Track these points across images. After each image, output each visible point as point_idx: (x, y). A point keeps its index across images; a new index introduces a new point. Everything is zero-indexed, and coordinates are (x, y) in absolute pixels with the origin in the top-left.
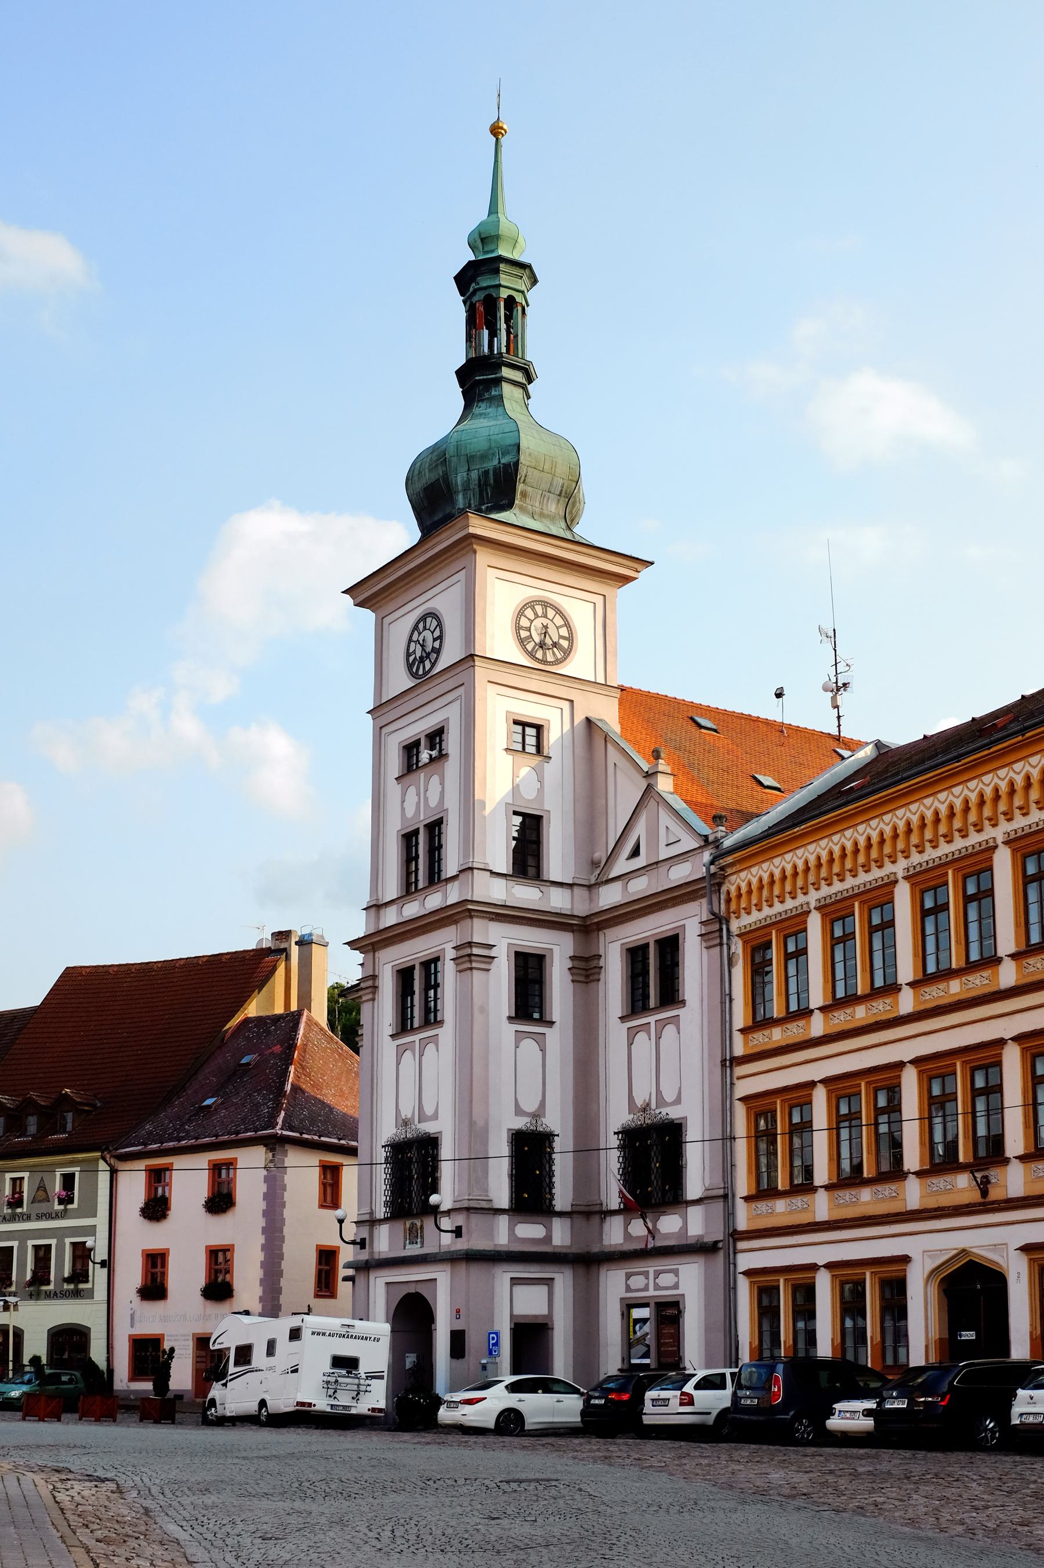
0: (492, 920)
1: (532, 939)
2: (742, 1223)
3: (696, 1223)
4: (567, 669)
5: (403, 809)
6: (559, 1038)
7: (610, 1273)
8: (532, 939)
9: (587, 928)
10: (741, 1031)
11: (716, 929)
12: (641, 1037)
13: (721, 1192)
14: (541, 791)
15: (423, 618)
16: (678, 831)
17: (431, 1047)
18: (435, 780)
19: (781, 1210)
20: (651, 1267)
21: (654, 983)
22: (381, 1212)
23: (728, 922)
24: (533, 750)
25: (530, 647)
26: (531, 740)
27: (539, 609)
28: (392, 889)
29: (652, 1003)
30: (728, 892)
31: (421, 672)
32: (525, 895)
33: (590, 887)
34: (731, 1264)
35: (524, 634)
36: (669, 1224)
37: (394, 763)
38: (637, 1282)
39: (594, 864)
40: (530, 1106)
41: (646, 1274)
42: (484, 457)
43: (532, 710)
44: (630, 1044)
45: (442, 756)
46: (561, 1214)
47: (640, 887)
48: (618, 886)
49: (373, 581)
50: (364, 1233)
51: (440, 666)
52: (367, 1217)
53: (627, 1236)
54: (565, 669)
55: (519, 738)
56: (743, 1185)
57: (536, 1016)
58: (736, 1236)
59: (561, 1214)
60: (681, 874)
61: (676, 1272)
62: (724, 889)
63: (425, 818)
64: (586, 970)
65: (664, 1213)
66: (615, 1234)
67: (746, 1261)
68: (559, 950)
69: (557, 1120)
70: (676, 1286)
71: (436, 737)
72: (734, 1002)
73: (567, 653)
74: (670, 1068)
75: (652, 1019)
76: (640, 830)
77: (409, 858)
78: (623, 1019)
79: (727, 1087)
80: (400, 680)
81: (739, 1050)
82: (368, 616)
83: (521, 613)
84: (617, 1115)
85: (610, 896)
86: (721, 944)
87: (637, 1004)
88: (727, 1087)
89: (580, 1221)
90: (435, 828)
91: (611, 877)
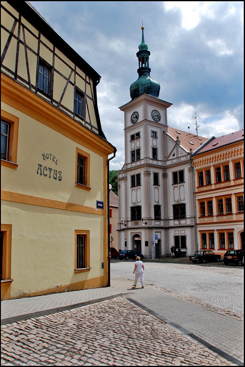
0: (150, 167)
1: (156, 171)
2: (198, 222)
3: (188, 222)
5: (131, 147)
6: (161, 188)
7: (171, 230)
8: (156, 171)
9: (165, 168)
10: (197, 188)
11: (191, 170)
12: (176, 188)
13: (194, 216)
14: (156, 144)
15: (134, 113)
16: (183, 152)
18: (138, 142)
19: (206, 220)
20: (180, 229)
21: (179, 178)
22: (130, 219)
23: (194, 168)
24: (154, 136)
26: (154, 135)
27: (155, 111)
28: (129, 161)
29: (178, 182)
30: (194, 163)
31: (134, 122)
32: (155, 162)
33: (165, 161)
34: (196, 230)
35: (153, 116)
36: (183, 222)
37: (129, 138)
38: (177, 232)
39: (166, 157)
40: (157, 201)
41: (179, 231)
42: (145, 84)
43: (155, 129)
44: (174, 189)
45: (139, 137)
46: (162, 220)
47: (175, 161)
48: (171, 161)
49: (125, 106)
50: (126, 223)
51: (138, 122)
52: (126, 220)
53: (174, 224)
54: (159, 122)
55: (152, 134)
56: (198, 214)
57: (157, 184)
58: (197, 224)
59: (162, 220)
60: (183, 159)
61: (185, 231)
62: (193, 162)
63: (136, 148)
64: (165, 176)
65: (182, 220)
66: (172, 223)
67: (199, 229)
68: (160, 173)
69: (161, 203)
70: (185, 233)
71: (138, 134)
72: (195, 183)
73: (160, 119)
74: (183, 193)
75: (178, 185)
76: (175, 151)
77: (133, 155)
78: (172, 185)
79: (194, 198)
80: (130, 124)
81: (197, 191)
82: (123, 112)
83: (152, 112)
84: (172, 203)
85: (169, 163)
86: (192, 172)
87: (175, 182)
88: (194, 198)
89: (165, 221)
90: (138, 151)
91: (169, 159)
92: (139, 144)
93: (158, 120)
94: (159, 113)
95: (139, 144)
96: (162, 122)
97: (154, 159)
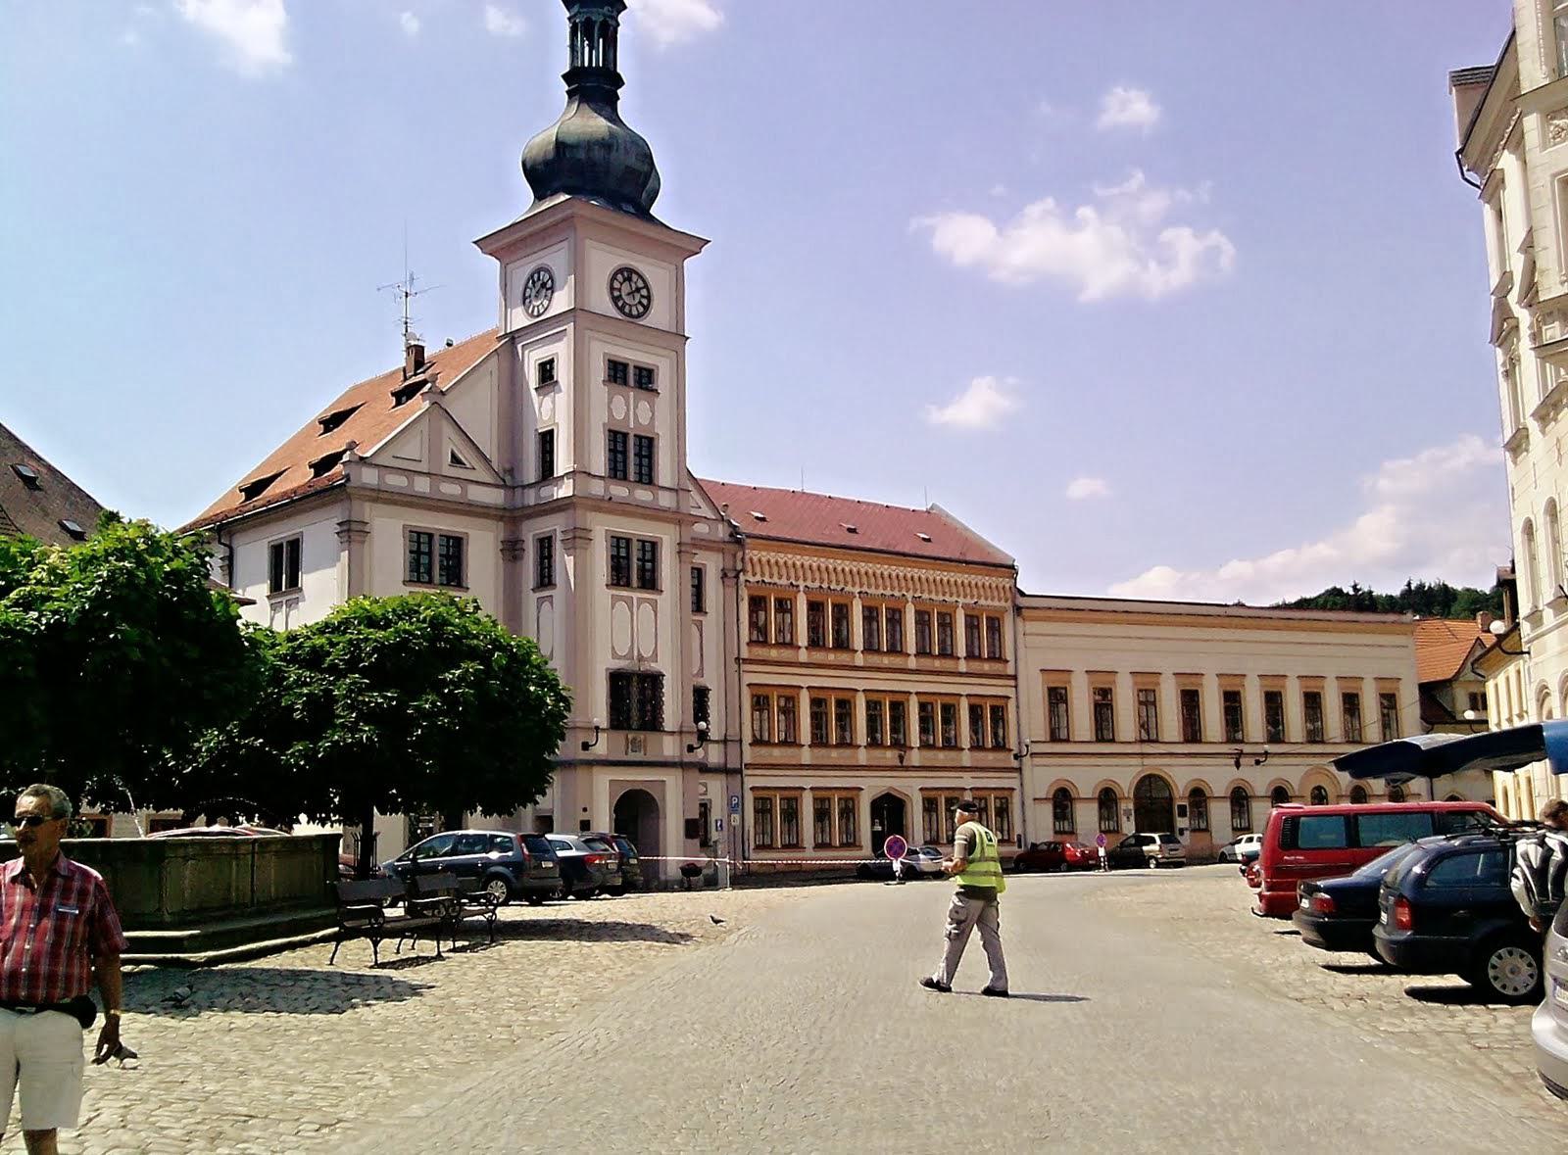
4: (648, 321)
17: (546, 605)
25: (620, 304)
73: (646, 308)
92: (554, 410)
93: (641, 309)
94: (644, 281)
95: (554, 410)
96: (659, 316)
97: (615, 477)
